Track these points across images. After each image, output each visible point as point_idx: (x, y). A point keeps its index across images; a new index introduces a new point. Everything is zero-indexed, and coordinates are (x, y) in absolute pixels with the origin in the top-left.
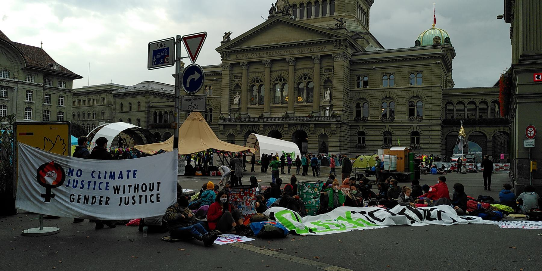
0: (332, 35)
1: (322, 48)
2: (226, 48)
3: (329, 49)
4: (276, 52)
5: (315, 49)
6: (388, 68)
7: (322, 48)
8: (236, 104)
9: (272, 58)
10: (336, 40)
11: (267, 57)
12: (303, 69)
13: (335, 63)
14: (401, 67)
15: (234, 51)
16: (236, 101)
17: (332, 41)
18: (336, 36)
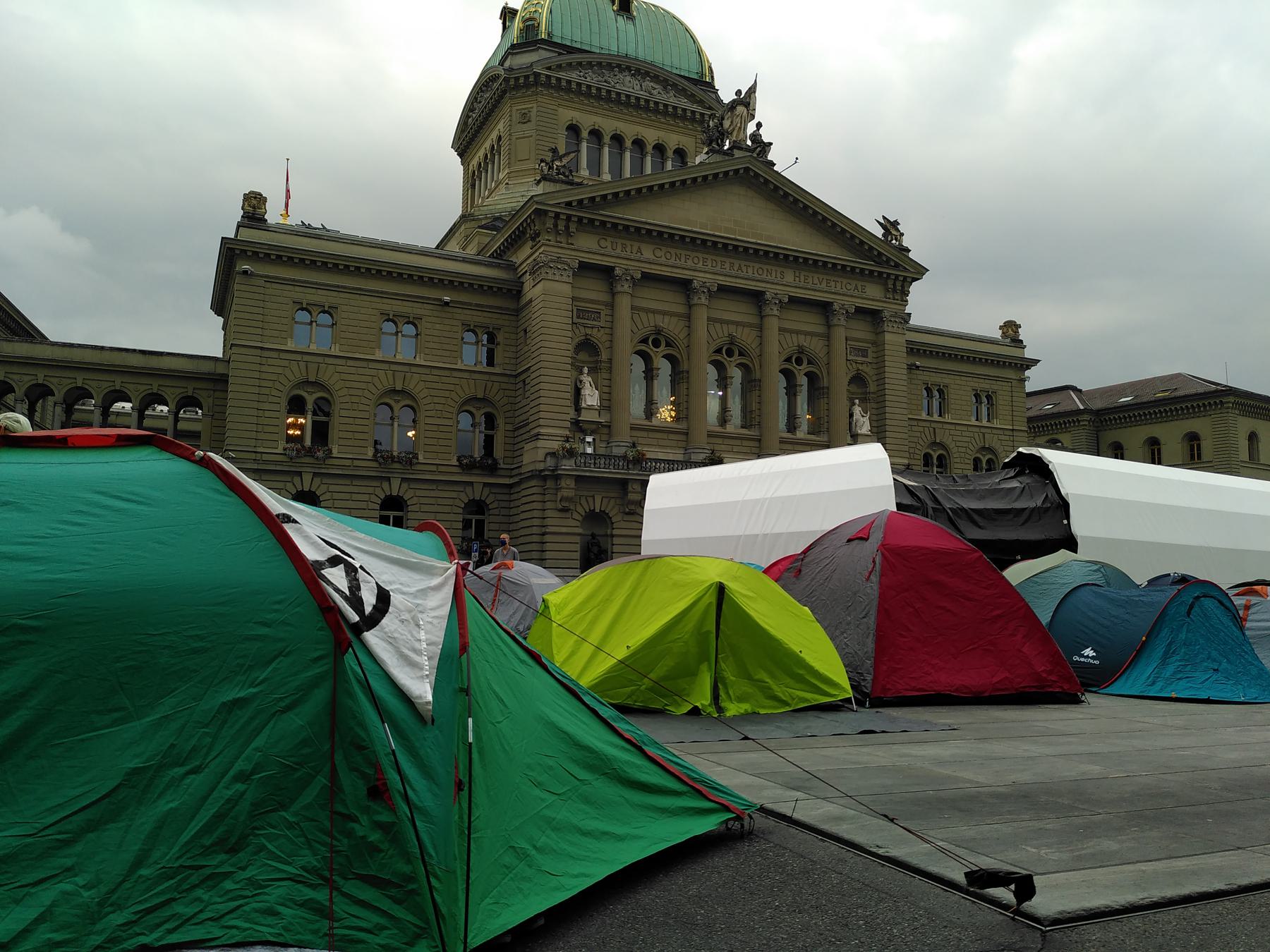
0: (889, 259)
1: (856, 288)
2: (569, 204)
3: (872, 295)
4: (732, 265)
5: (839, 285)
6: (937, 371)
7: (856, 288)
8: (590, 408)
9: (722, 280)
10: (897, 276)
11: (706, 272)
12: (798, 332)
13: (888, 337)
14: (960, 374)
15: (603, 223)
16: (591, 397)
17: (889, 275)
18: (897, 266)
